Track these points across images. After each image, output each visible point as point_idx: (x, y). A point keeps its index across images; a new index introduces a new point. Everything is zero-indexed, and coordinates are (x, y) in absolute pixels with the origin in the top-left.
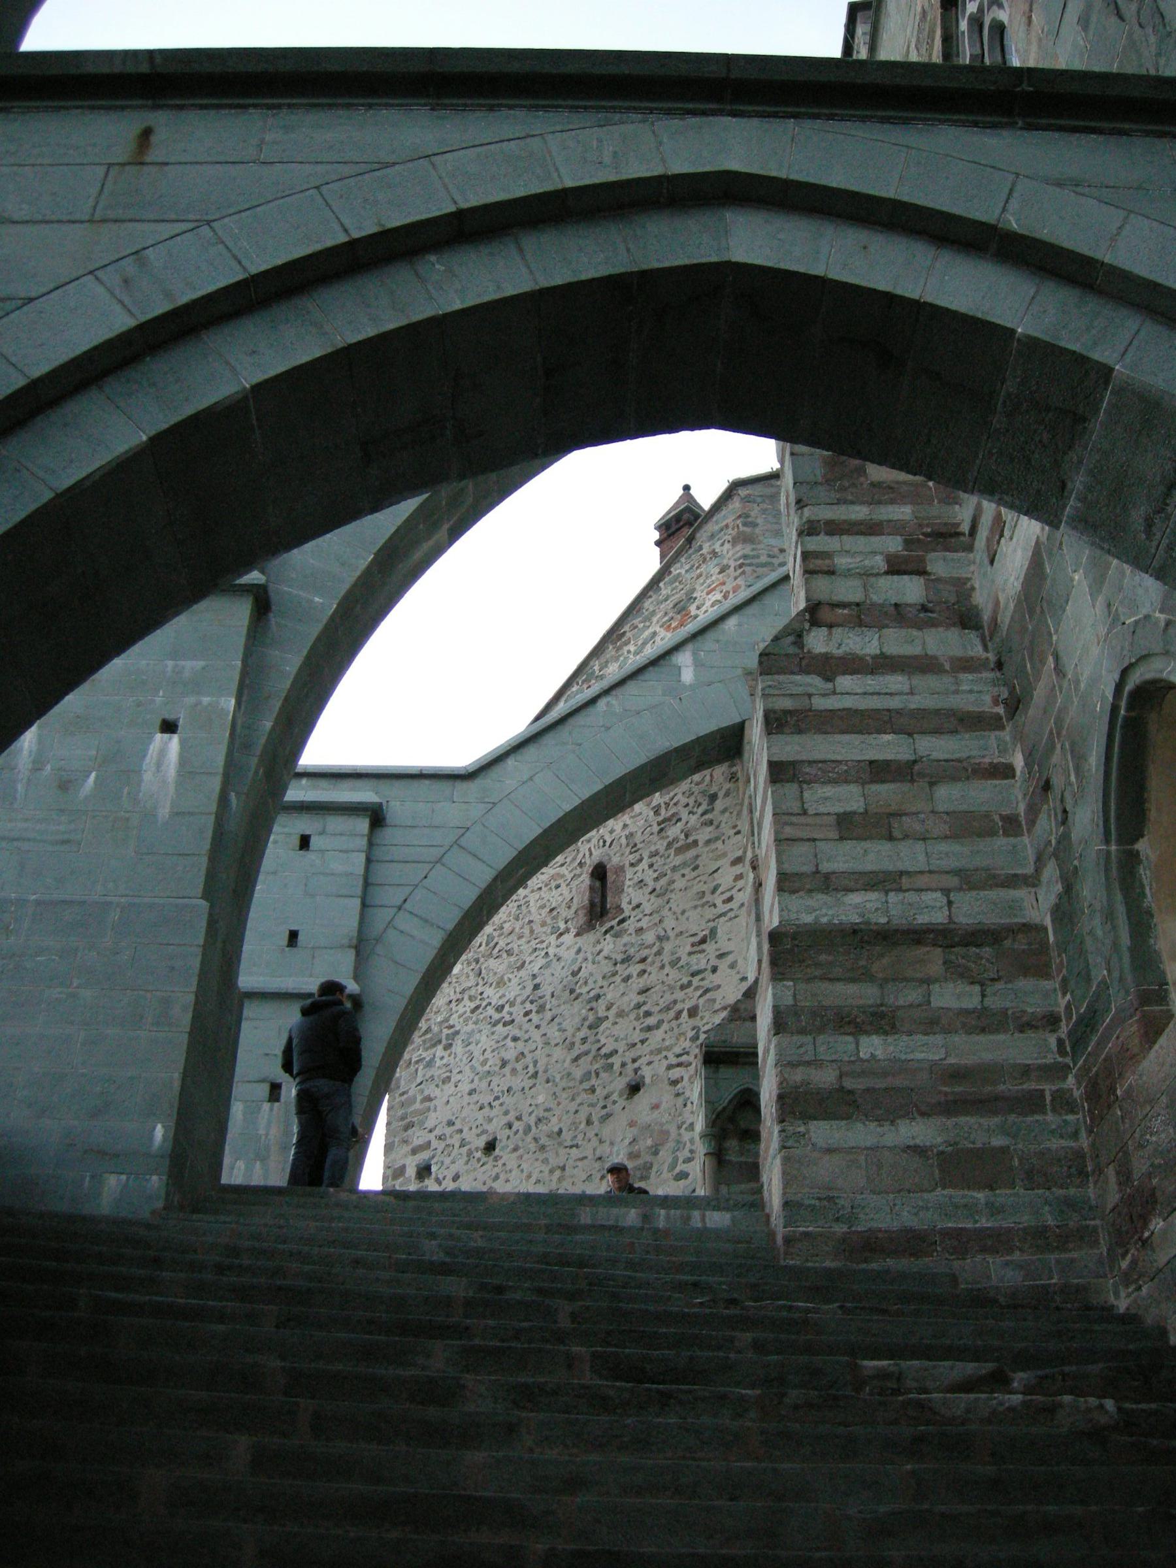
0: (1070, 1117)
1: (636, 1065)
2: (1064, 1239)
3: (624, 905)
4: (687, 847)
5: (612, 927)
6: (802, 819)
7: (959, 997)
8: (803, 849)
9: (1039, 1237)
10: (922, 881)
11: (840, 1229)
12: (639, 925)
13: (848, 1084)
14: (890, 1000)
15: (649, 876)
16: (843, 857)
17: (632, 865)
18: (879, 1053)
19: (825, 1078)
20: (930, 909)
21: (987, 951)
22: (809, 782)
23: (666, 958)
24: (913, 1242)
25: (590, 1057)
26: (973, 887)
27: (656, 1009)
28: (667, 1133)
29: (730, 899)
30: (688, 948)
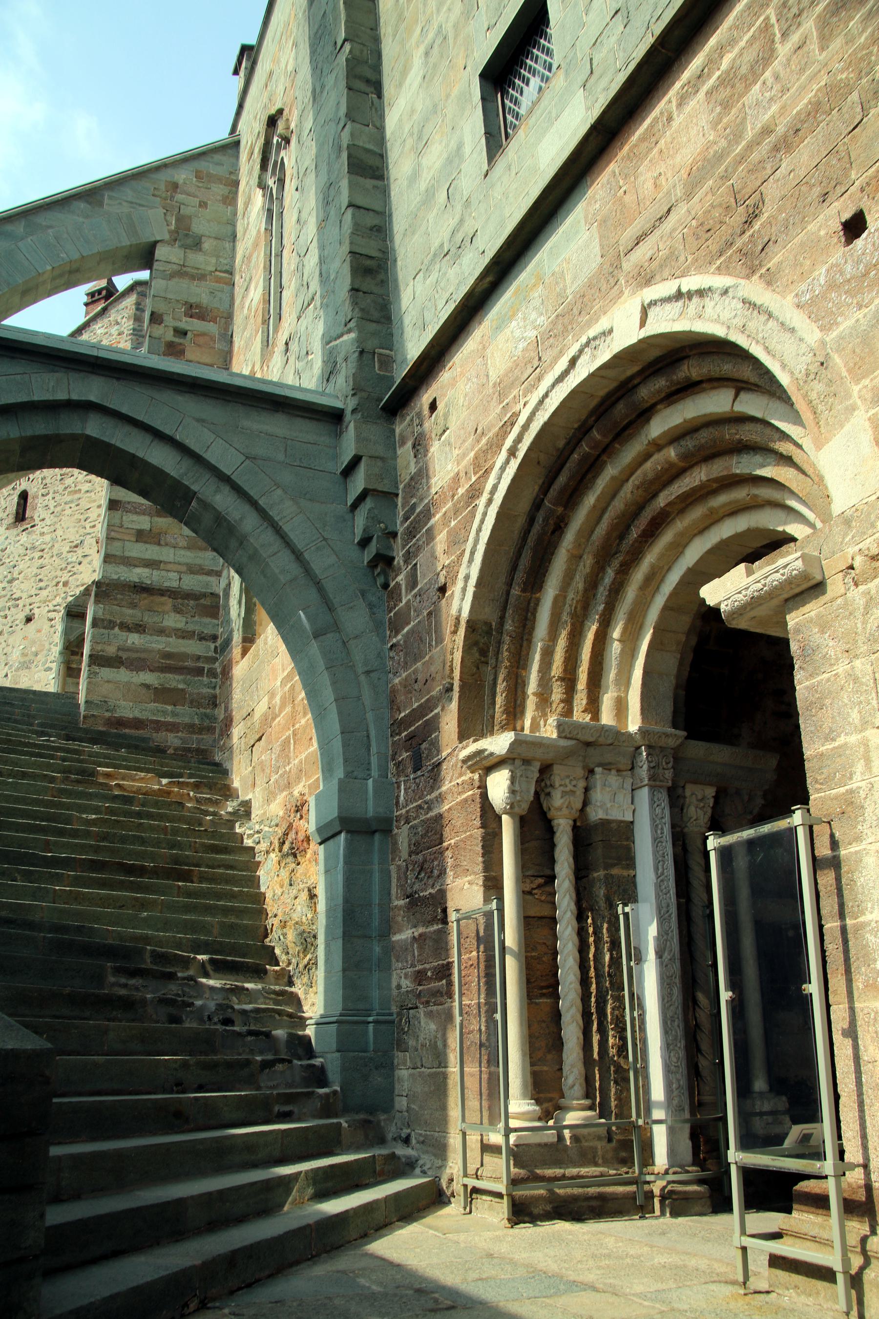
0: (213, 680)
2: (201, 730)
3: (36, 517)
4: (75, 492)
6: (120, 530)
7: (176, 622)
8: (118, 544)
9: (191, 728)
10: (169, 567)
11: (108, 714)
12: (43, 530)
13: (120, 654)
14: (146, 619)
15: (52, 504)
16: (137, 550)
17: (43, 495)
18: (136, 642)
20: (171, 580)
21: (192, 603)
22: (127, 512)
24: (138, 723)
25: (6, 599)
26: (192, 573)
27: (45, 579)
29: (94, 526)
30: (68, 549)
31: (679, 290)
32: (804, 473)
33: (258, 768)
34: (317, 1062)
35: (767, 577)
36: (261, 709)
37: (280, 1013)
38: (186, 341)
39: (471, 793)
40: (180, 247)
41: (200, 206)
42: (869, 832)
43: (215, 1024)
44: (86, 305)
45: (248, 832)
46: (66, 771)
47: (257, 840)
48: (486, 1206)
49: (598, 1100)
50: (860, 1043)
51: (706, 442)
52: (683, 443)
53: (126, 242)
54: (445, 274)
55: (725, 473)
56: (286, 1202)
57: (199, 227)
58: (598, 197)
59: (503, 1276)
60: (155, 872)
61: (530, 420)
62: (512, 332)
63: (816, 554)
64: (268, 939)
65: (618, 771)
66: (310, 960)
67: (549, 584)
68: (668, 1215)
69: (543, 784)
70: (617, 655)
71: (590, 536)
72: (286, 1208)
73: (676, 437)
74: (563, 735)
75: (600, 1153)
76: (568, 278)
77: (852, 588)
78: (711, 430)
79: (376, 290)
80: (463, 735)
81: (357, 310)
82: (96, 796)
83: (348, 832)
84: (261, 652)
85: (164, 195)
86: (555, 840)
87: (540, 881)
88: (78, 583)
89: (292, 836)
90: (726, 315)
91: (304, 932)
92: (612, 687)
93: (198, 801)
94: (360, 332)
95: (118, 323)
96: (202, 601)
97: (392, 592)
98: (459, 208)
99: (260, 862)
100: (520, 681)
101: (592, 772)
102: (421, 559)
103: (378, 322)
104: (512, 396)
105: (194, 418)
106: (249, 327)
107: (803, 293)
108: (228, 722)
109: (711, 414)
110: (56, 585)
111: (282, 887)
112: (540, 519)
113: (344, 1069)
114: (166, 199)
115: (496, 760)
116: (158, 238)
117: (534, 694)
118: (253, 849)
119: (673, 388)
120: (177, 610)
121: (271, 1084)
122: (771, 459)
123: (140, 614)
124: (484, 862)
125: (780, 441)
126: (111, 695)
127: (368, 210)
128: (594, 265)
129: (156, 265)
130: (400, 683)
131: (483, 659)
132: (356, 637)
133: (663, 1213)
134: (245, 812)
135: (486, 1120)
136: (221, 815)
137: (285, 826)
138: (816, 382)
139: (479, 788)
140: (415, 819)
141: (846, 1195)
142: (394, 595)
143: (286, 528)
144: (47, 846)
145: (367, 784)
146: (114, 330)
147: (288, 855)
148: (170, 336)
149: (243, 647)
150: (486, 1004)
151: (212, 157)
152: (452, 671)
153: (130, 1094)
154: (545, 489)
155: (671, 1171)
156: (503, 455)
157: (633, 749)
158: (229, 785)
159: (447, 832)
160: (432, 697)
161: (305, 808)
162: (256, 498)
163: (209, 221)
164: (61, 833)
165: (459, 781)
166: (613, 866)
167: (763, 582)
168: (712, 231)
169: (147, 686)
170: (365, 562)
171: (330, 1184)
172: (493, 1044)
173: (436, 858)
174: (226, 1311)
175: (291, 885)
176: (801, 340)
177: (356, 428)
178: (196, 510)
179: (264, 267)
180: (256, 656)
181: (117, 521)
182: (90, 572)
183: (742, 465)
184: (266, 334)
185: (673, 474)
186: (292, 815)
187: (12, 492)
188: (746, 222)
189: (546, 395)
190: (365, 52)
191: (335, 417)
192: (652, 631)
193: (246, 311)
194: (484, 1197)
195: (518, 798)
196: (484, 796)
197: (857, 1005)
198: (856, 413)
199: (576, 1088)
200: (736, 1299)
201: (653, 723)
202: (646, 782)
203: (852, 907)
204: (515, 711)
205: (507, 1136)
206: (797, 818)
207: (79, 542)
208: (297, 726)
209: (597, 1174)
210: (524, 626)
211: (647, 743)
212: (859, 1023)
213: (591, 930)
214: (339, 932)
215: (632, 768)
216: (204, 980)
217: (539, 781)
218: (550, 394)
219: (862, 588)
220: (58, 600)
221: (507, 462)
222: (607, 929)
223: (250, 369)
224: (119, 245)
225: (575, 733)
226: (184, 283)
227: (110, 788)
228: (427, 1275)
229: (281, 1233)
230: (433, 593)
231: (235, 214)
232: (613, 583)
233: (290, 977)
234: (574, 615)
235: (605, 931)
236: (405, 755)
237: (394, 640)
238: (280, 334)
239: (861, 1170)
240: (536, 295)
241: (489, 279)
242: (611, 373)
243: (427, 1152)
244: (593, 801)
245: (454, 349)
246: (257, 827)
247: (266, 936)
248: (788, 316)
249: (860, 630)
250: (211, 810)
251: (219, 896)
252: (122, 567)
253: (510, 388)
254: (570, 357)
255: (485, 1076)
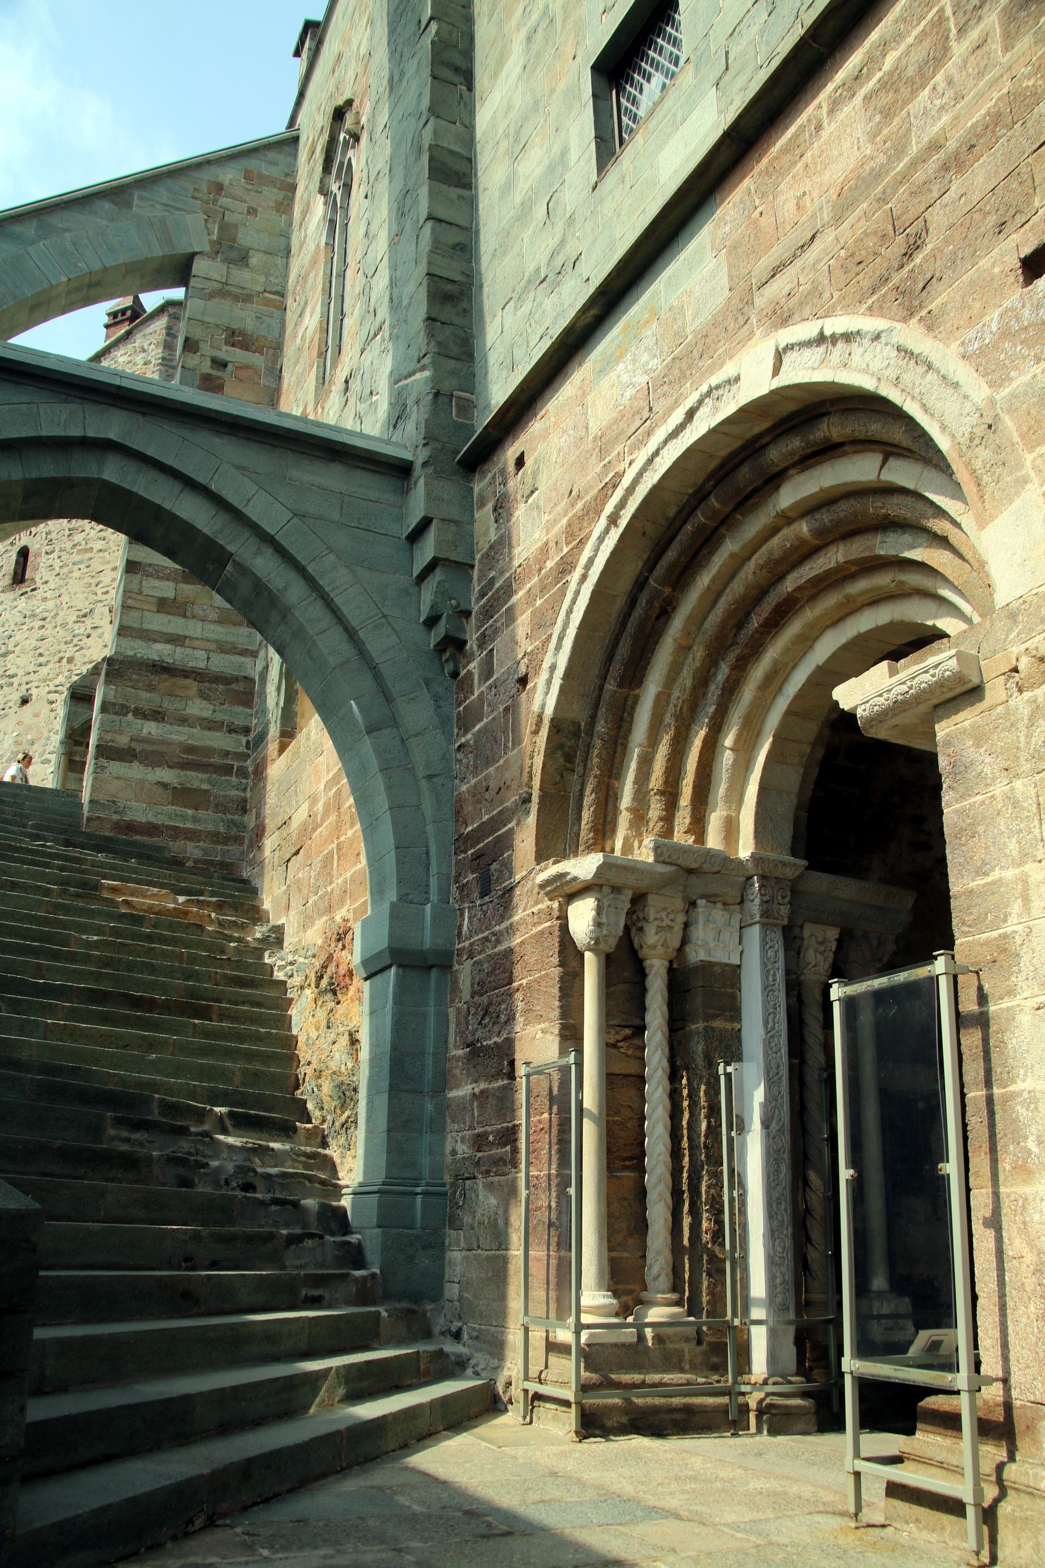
0: (244, 781)
1: (29, 686)
2: (227, 840)
3: (37, 579)
4: (86, 551)
5: (27, 592)
6: (139, 597)
9: (215, 837)
10: (196, 643)
12: (45, 595)
13: (134, 745)
15: (57, 564)
16: (159, 622)
17: (47, 553)
19: (123, 741)
20: (197, 659)
23: (59, 620)
24: (152, 829)
26: (223, 652)
27: (46, 653)
28: (42, 733)
29: (107, 593)
30: (74, 618)
31: (821, 333)
32: (961, 556)
33: (294, 888)
34: (354, 1238)
35: (913, 678)
36: (300, 816)
37: (310, 1179)
38: (226, 375)
39: (548, 924)
40: (223, 261)
41: (249, 213)
42: (1024, 985)
43: (234, 1189)
44: (107, 326)
45: (280, 963)
46: (64, 882)
47: (290, 973)
48: (550, 1415)
49: (687, 1294)
50: (1004, 1234)
51: (845, 516)
52: (817, 516)
53: (158, 252)
54: (541, 304)
55: (867, 554)
56: (312, 1403)
57: (247, 237)
58: (728, 218)
59: (569, 1499)
60: (166, 1007)
61: (636, 482)
62: (619, 377)
63: (974, 652)
64: (299, 1091)
65: (725, 904)
66: (349, 1117)
67: (651, 678)
68: (765, 1432)
69: (635, 917)
70: (729, 767)
72: (312, 1411)
73: (809, 509)
74: (661, 859)
75: (687, 1357)
76: (689, 314)
77: (1015, 695)
78: (852, 501)
79: (456, 320)
80: (542, 856)
81: (433, 344)
82: (99, 913)
83: (399, 966)
84: (302, 749)
85: (205, 198)
86: (647, 984)
87: (628, 1032)
88: (86, 660)
89: (332, 968)
90: (876, 365)
91: (342, 1083)
92: (721, 804)
93: (221, 924)
94: (435, 370)
95: (144, 351)
96: (234, 686)
97: (462, 682)
98: (560, 226)
99: (292, 999)
100: (611, 793)
101: (693, 904)
102: (498, 644)
103: (457, 359)
104: (616, 453)
105: (233, 465)
106: (302, 360)
107: (970, 341)
108: (260, 832)
109: (853, 483)
110: (59, 662)
111: (317, 1029)
112: (643, 601)
113: (385, 1248)
114: (207, 203)
115: (580, 886)
116: (197, 250)
117: (628, 809)
118: (285, 983)
119: (809, 451)
120: (203, 696)
121: (298, 1262)
122: (922, 539)
123: (158, 699)
124: (561, 1007)
125: (934, 518)
126: (120, 794)
127: (451, 224)
128: (720, 300)
129: (193, 282)
130: (468, 791)
131: (568, 765)
132: (416, 735)
133: (759, 1431)
134: (276, 939)
135: (552, 1314)
136: (248, 942)
137: (323, 957)
138: (982, 448)
139: (558, 918)
140: (480, 953)
141: (981, 1414)
142: (465, 686)
143: (339, 601)
144: (39, 971)
145: (424, 910)
146: (139, 359)
147: (326, 991)
148: (206, 367)
149: (281, 742)
150: (557, 1176)
151: (266, 155)
152: (531, 778)
153: (130, 1269)
154: (651, 565)
155: (770, 1381)
156: (603, 522)
157: (742, 879)
158: (258, 907)
159: (518, 970)
160: (506, 808)
161: (349, 936)
162: (303, 563)
163: (258, 231)
164: (56, 956)
165: (535, 910)
166: (714, 1017)
167: (909, 683)
168: (864, 264)
169: (164, 785)
170: (432, 646)
171: (365, 1384)
172: (565, 1224)
173: (503, 1001)
174: (239, 1530)
175: (329, 1027)
176: (966, 397)
177: (426, 485)
178: (232, 575)
179: (323, 289)
180: (296, 753)
181: (135, 586)
182: (100, 646)
183: (887, 545)
184: (322, 370)
185: (804, 553)
186: (333, 945)
187: (10, 548)
188: (905, 254)
189: (656, 453)
190: (455, 34)
191: (400, 471)
192: (771, 739)
193: (298, 341)
194: (548, 1405)
195: (605, 932)
196: (564, 929)
197: (1002, 1190)
198: (1028, 487)
199: (661, 1279)
200: (846, 1534)
201: (769, 849)
202: (757, 919)
203: (1001, 1073)
204: (604, 829)
205: (577, 1334)
206: (940, 965)
207: (88, 610)
208: (342, 839)
209: (684, 1381)
210: (619, 728)
211: (760, 872)
212: (1004, 1211)
213: (685, 1092)
214: (385, 1084)
215: (742, 902)
216: (221, 1137)
217: (630, 913)
218: (661, 452)
219: (1027, 695)
220: (61, 679)
221: (607, 531)
222: (705, 1092)
223: (301, 410)
224: (149, 256)
225: (676, 857)
226: (226, 305)
227: (116, 905)
228: (478, 1494)
229: (306, 1439)
230: (512, 685)
231: (290, 224)
232: (727, 680)
233: (324, 1137)
234: (679, 717)
235: (702, 1094)
236: (471, 877)
237: (463, 740)
238: (339, 369)
239: (1000, 1385)
240: (650, 333)
241: (593, 312)
242: (736, 430)
243: (481, 1350)
244: (694, 939)
245: (548, 394)
246: (290, 958)
247: (297, 1087)
248: (951, 370)
249: (1022, 745)
250: (236, 935)
251: (241, 1037)
252: (139, 641)
253: (614, 443)
254: (687, 408)
255: (553, 1262)
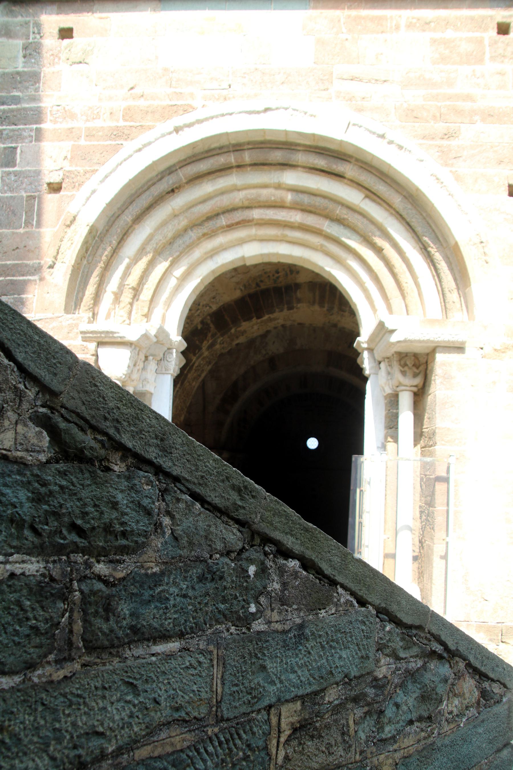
52: (301, 196)
55: (318, 226)
71: (190, 208)
78: (326, 201)
139: (93, 355)
185: (280, 206)
202: (172, 372)
